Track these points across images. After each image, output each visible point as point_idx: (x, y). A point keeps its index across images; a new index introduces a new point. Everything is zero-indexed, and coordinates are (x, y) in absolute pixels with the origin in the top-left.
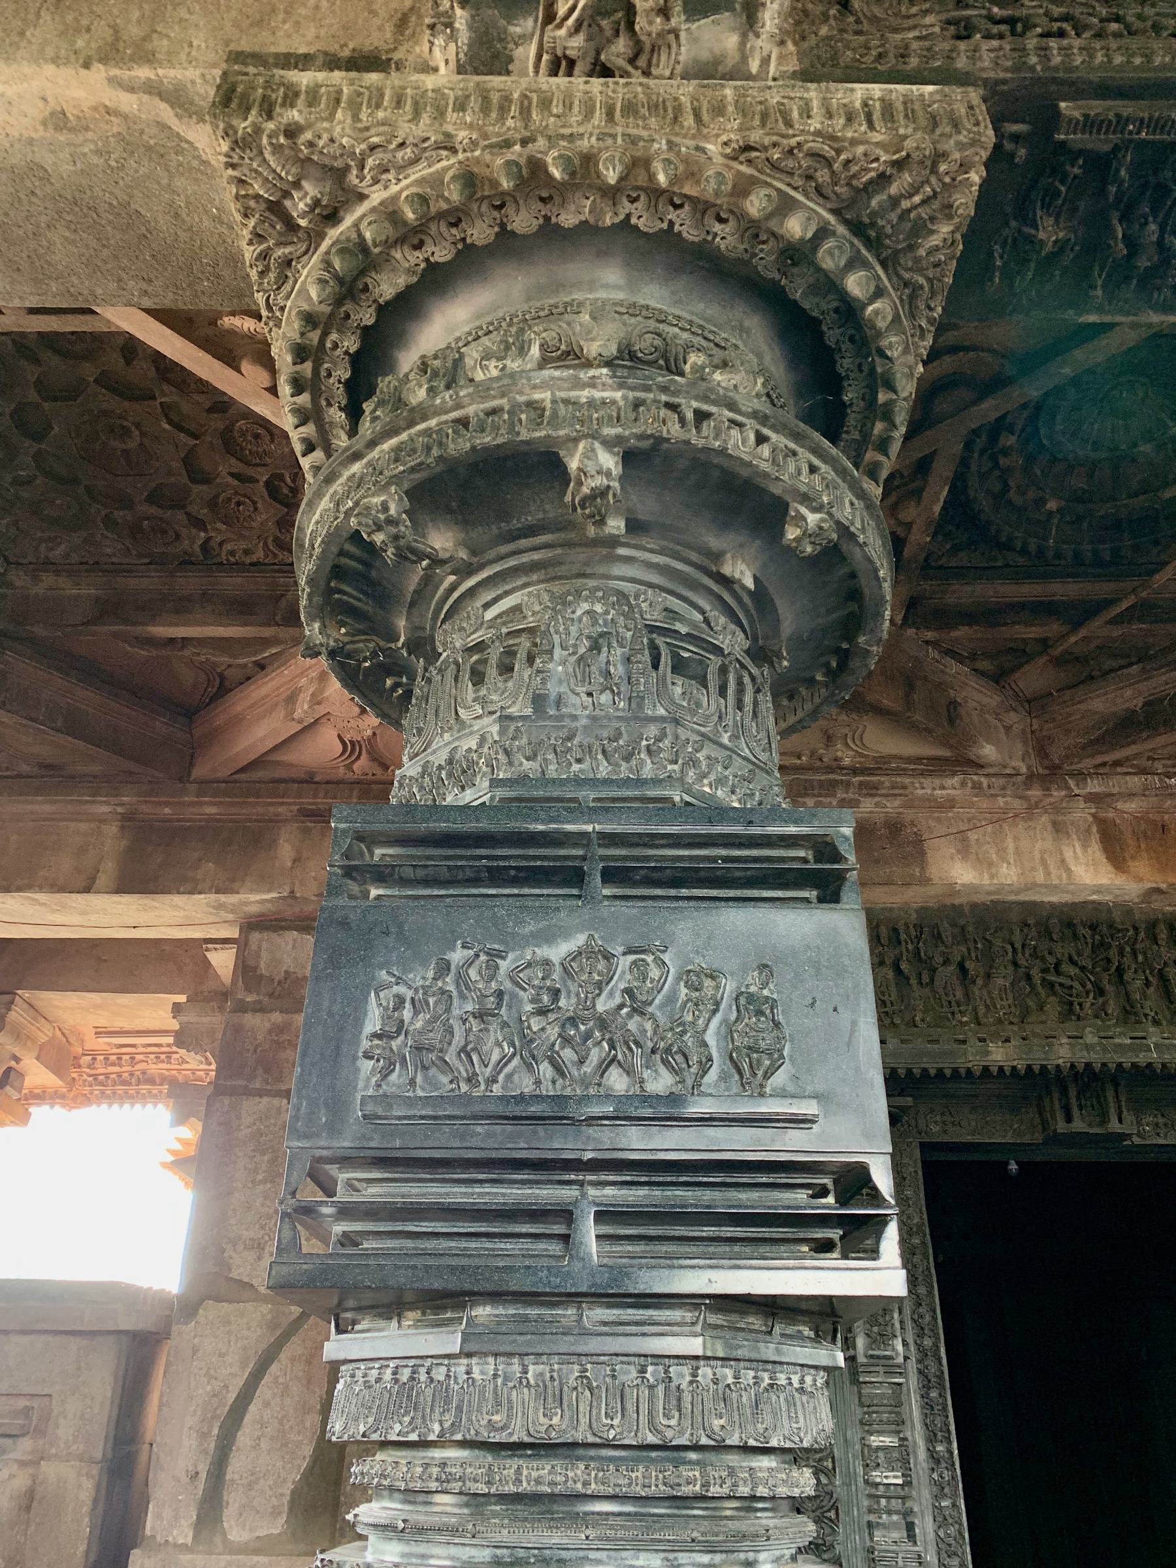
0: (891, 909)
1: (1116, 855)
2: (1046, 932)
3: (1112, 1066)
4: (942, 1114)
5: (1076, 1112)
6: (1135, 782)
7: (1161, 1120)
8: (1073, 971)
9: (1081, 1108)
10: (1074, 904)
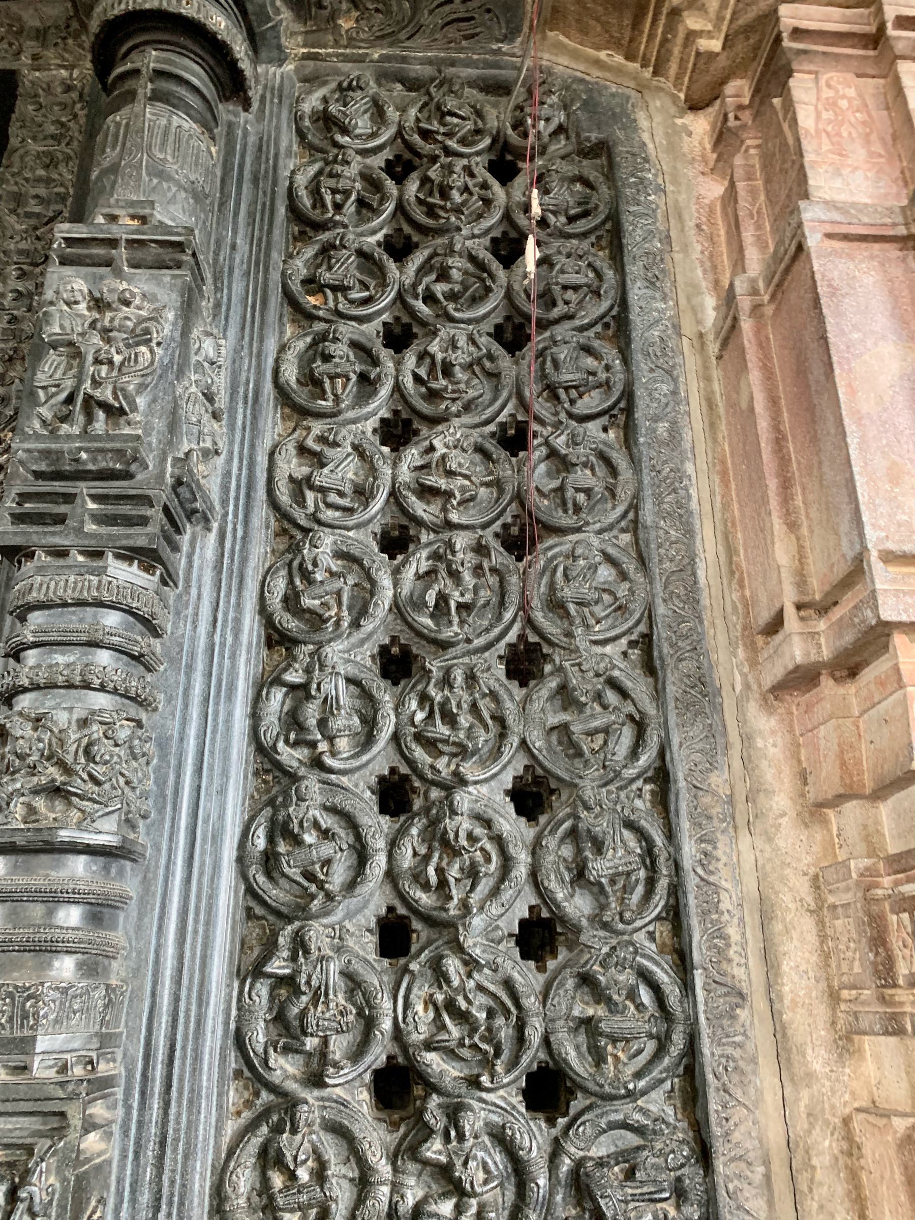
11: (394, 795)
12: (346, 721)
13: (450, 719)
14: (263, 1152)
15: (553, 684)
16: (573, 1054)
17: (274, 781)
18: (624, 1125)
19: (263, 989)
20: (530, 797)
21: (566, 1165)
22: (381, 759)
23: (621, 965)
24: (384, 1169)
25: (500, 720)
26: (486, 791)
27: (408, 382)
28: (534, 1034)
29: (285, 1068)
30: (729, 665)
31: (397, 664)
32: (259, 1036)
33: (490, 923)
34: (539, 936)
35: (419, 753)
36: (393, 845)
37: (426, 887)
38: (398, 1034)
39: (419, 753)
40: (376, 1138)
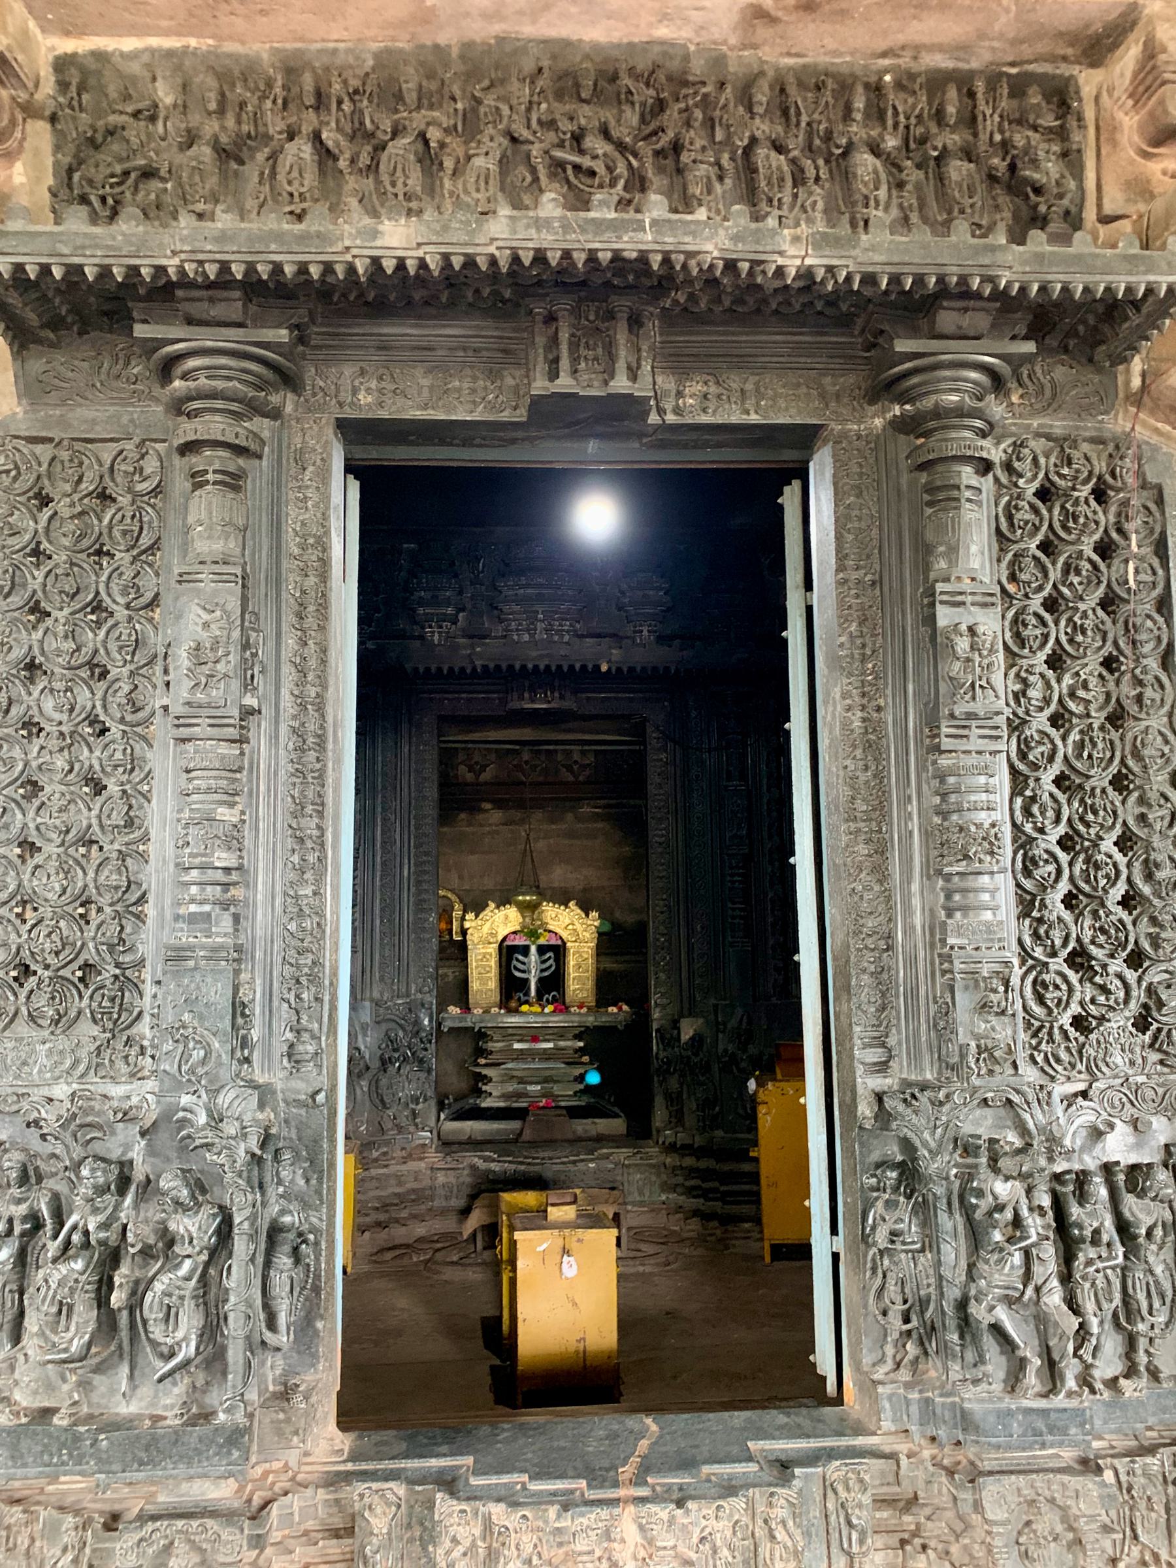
0: (335, 51)
3: (580, 258)
4: (380, 379)
5: (565, 364)
7: (713, 389)
8: (600, 146)
9: (575, 361)
10: (631, 45)
12: (1050, 814)
13: (1095, 813)
14: (1035, 982)
15: (1136, 794)
16: (1146, 945)
18: (1166, 971)
19: (1027, 922)
20: (1125, 843)
21: (1144, 984)
22: (1062, 829)
23: (1167, 913)
24: (1077, 984)
25: (1115, 813)
27: (1063, 639)
28: (1132, 940)
29: (1038, 952)
32: (1028, 940)
34: (1126, 902)
35: (1081, 828)
36: (1071, 864)
37: (1088, 882)
38: (1079, 940)
39: (1081, 828)
40: (1073, 977)
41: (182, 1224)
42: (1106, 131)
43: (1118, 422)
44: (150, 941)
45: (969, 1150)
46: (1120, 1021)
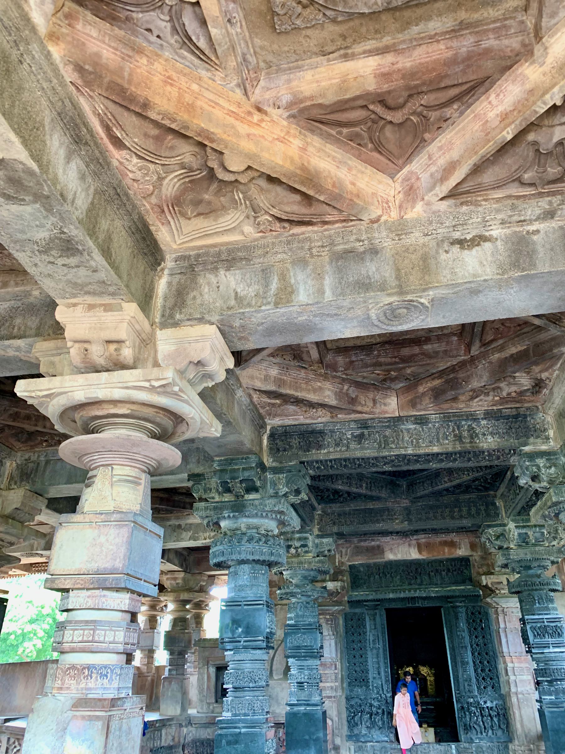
1: (420, 552)
2: (407, 567)
6: (423, 536)
11: (480, 662)
17: (474, 662)
26: (486, 662)
30: (499, 655)
31: (479, 654)
33: (487, 670)
34: (490, 670)
41: (379, 711)
42: (474, 565)
43: (479, 604)
44: (370, 676)
45: (468, 703)
46: (489, 688)
